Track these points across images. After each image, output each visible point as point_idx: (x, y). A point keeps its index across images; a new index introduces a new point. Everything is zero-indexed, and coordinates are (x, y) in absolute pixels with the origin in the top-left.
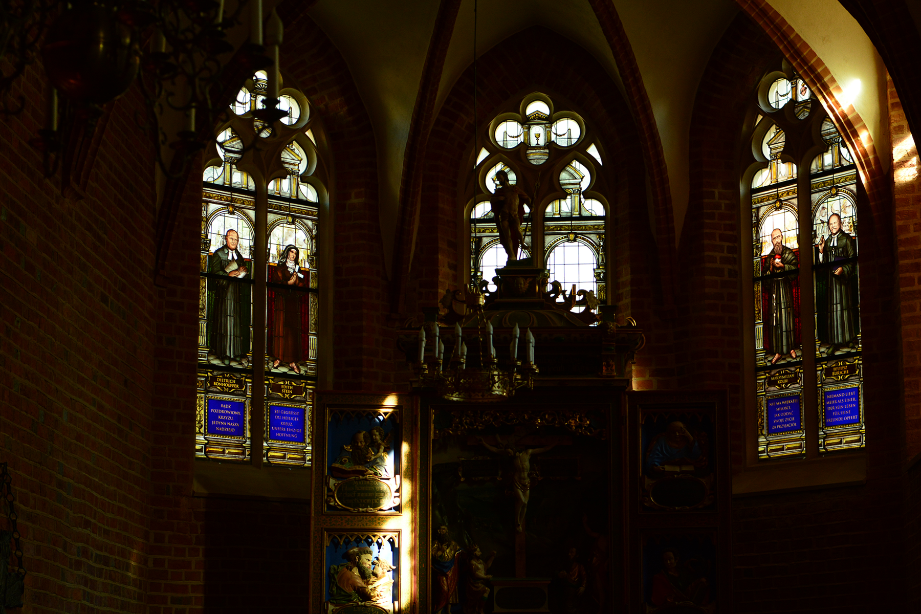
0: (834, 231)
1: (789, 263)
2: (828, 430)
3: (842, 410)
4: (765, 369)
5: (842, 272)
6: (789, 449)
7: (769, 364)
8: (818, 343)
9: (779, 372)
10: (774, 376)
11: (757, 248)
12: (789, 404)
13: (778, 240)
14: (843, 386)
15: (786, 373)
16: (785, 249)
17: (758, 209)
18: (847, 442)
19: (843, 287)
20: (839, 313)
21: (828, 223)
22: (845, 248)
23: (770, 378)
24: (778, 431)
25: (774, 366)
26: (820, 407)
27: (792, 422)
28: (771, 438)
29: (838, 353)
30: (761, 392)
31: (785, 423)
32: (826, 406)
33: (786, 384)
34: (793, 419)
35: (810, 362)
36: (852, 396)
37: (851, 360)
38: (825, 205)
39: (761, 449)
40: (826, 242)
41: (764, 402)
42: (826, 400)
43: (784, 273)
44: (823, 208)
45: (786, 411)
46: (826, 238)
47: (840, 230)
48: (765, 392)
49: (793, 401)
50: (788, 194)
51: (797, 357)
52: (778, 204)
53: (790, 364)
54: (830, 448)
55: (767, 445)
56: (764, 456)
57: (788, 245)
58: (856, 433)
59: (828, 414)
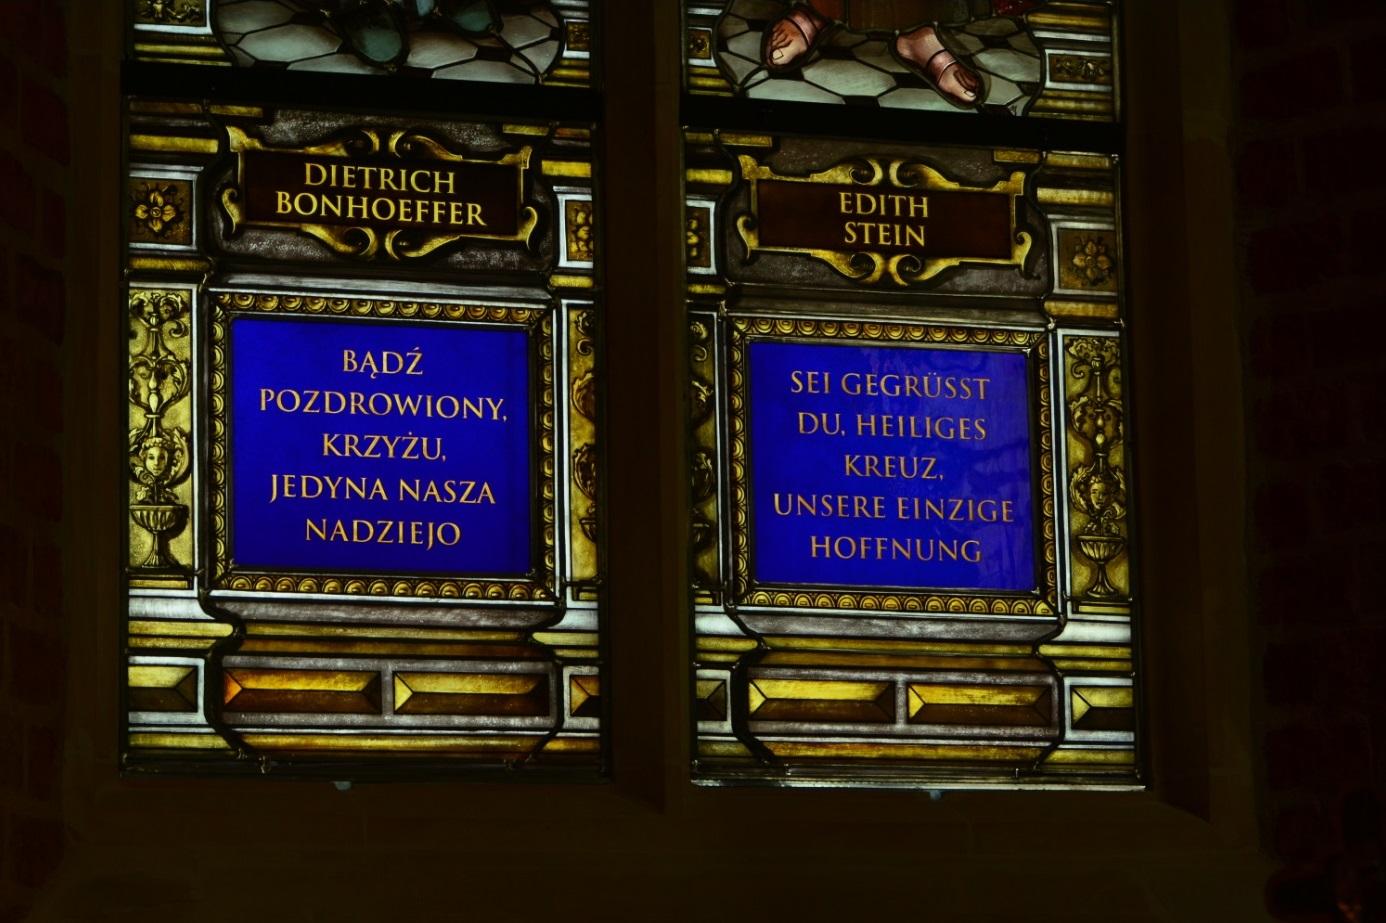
37: (973, 164)
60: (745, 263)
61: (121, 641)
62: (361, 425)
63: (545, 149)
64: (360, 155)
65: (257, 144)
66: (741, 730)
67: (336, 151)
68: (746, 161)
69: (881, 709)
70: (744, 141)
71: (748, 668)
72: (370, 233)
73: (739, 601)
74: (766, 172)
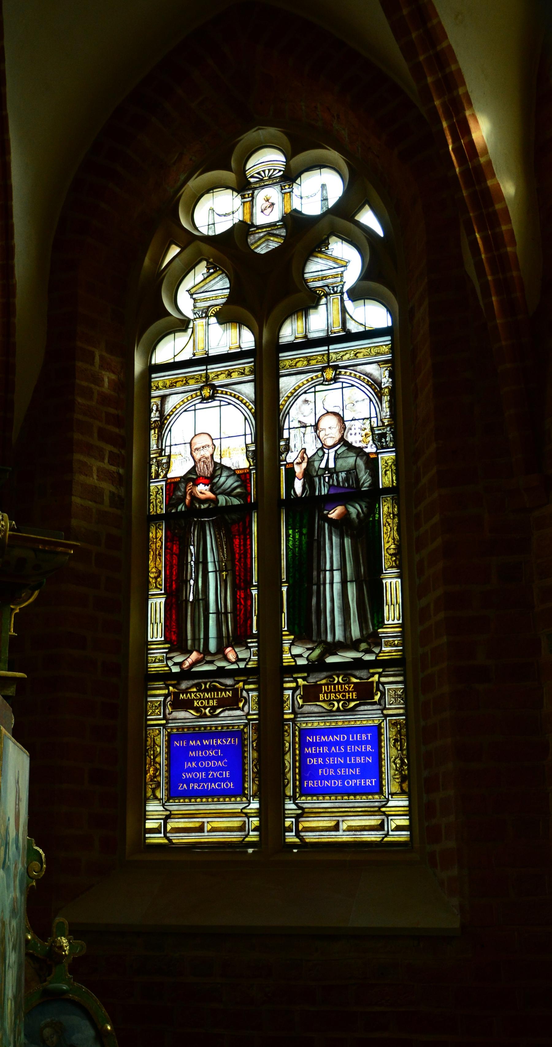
0: (330, 442)
1: (228, 493)
2: (308, 802)
3: (340, 766)
4: (166, 677)
5: (346, 516)
6: (213, 830)
7: (175, 669)
8: (287, 639)
9: (198, 685)
10: (185, 691)
11: (159, 464)
12: (219, 747)
13: (207, 453)
14: (341, 721)
15: (214, 689)
16: (219, 468)
17: (163, 398)
18: (350, 829)
19: (347, 542)
20: (337, 587)
21: (316, 427)
22: (352, 472)
23: (176, 695)
24: (190, 795)
25: (186, 674)
26: (288, 758)
27: (224, 780)
28: (174, 807)
29: (331, 660)
30: (155, 717)
31: (206, 780)
32: (304, 757)
33: (214, 708)
34: (226, 774)
35: (269, 675)
36: (366, 742)
37: (363, 673)
38: (310, 397)
39: (150, 825)
40: (310, 462)
41: (162, 740)
42: (303, 744)
43: (214, 510)
44: (306, 401)
45: (210, 758)
46: (310, 453)
47: (343, 441)
48: (163, 719)
49: (229, 741)
50: (229, 375)
51: (238, 660)
52: (207, 392)
53: (222, 673)
54: (310, 837)
55: (166, 819)
56: (157, 839)
57: (226, 462)
58: (372, 813)
59: (307, 772)
60: (299, 708)
61: (143, 816)
62: (210, 758)
63: (246, 683)
64: (199, 690)
65: (176, 691)
66: (297, 835)
67: (195, 690)
68: (300, 681)
69: (336, 828)
70: (300, 675)
71: (298, 817)
72: (202, 709)
73: (296, 799)
74: (305, 683)
